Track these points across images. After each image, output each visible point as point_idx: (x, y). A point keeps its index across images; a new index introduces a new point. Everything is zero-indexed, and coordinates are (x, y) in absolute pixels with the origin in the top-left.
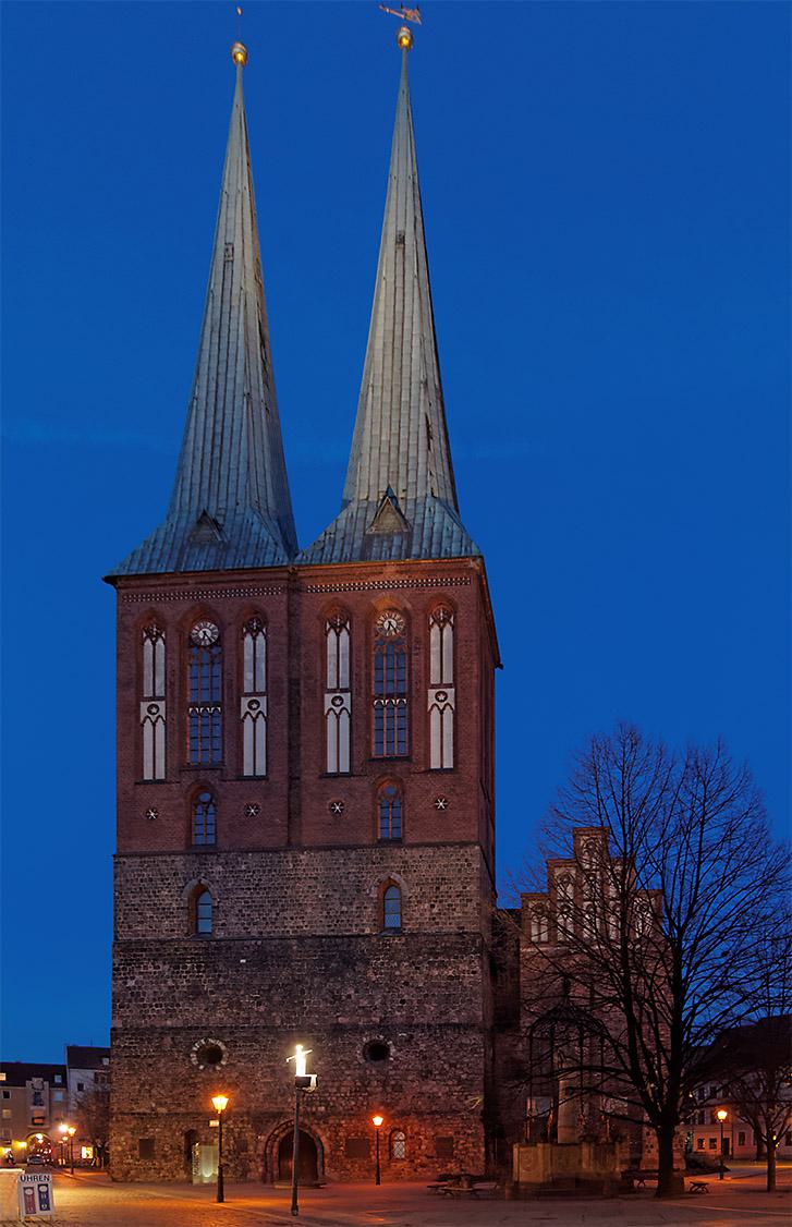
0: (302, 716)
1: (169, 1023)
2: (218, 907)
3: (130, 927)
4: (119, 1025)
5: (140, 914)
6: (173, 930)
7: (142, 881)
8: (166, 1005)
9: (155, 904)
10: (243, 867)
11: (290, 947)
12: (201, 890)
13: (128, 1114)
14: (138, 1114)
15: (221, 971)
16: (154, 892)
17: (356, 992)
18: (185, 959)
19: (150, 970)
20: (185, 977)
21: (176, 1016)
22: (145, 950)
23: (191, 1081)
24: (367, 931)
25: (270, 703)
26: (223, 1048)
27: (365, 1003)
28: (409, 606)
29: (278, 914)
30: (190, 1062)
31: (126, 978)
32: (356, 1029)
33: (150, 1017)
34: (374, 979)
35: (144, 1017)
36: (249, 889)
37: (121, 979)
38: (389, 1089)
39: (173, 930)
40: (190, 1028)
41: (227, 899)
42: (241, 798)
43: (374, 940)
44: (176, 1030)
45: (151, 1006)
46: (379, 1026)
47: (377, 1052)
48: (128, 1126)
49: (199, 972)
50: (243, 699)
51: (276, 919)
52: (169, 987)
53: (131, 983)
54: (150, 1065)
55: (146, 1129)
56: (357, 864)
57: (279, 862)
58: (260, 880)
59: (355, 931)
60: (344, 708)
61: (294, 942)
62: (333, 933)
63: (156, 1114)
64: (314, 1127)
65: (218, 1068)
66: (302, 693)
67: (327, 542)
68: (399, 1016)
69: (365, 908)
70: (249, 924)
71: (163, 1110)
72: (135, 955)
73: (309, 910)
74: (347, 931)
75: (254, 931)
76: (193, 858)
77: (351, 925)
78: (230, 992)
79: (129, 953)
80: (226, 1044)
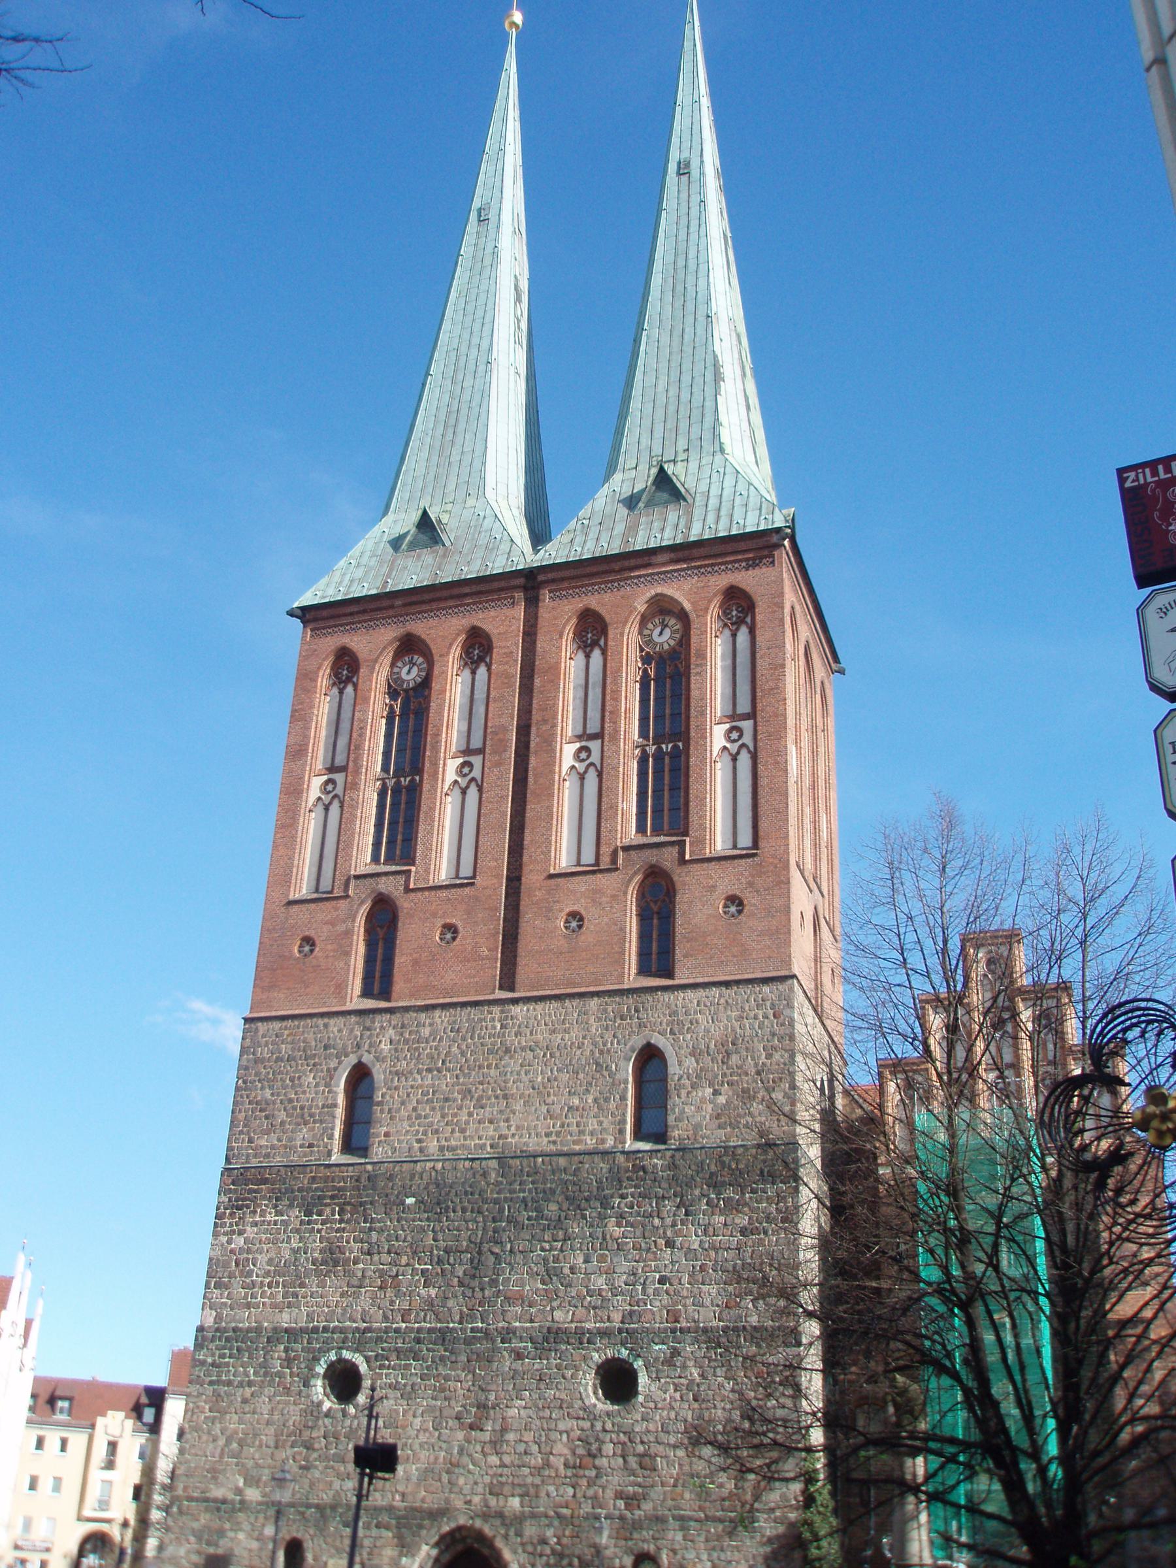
0: (531, 780)
1: (285, 1319)
2: (380, 1104)
3: (250, 1141)
4: (210, 1322)
5: (267, 1117)
6: (311, 1146)
7: (278, 1059)
8: (284, 1286)
9: (290, 1101)
10: (426, 1032)
11: (485, 1174)
12: (360, 1076)
13: (197, 1500)
14: (215, 1500)
15: (372, 1221)
16: (292, 1080)
17: (586, 1261)
18: (324, 1197)
19: (268, 1218)
20: (319, 1231)
21: (299, 1307)
22: (265, 1181)
23: (306, 1434)
24: (610, 1142)
25: (487, 764)
26: (363, 1368)
27: (600, 1282)
28: (687, 606)
29: (470, 1114)
30: (308, 1396)
31: (233, 1232)
32: (582, 1338)
33: (257, 1306)
34: (616, 1235)
35: (248, 1306)
36: (429, 1070)
37: (225, 1234)
38: (633, 1462)
39: (311, 1146)
40: (315, 1330)
41: (396, 1088)
42: (434, 915)
43: (621, 1158)
44: (292, 1334)
45: (262, 1284)
46: (620, 1331)
47: (618, 1382)
48: (196, 1525)
49: (341, 1221)
50: (449, 762)
51: (467, 1123)
52: (293, 1249)
53: (239, 1242)
54: (245, 1401)
55: (221, 1533)
56: (600, 1019)
57: (480, 1020)
58: (448, 1054)
59: (590, 1142)
60: (592, 764)
61: (494, 1164)
62: (553, 1147)
63: (242, 1502)
64: (499, 1543)
65: (352, 1410)
66: (532, 745)
67: (578, 532)
68: (656, 1308)
69: (607, 1100)
70: (425, 1133)
71: (253, 1495)
72: (251, 1191)
73: (518, 1106)
74: (575, 1143)
75: (433, 1145)
76: (353, 1019)
77: (581, 1132)
78: (386, 1258)
79: (243, 1187)
80: (368, 1360)
